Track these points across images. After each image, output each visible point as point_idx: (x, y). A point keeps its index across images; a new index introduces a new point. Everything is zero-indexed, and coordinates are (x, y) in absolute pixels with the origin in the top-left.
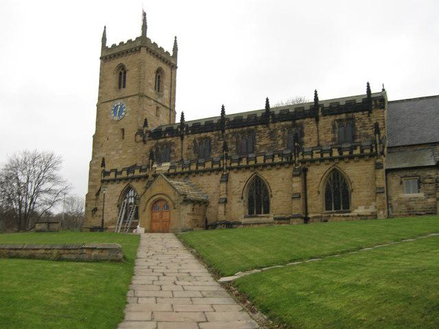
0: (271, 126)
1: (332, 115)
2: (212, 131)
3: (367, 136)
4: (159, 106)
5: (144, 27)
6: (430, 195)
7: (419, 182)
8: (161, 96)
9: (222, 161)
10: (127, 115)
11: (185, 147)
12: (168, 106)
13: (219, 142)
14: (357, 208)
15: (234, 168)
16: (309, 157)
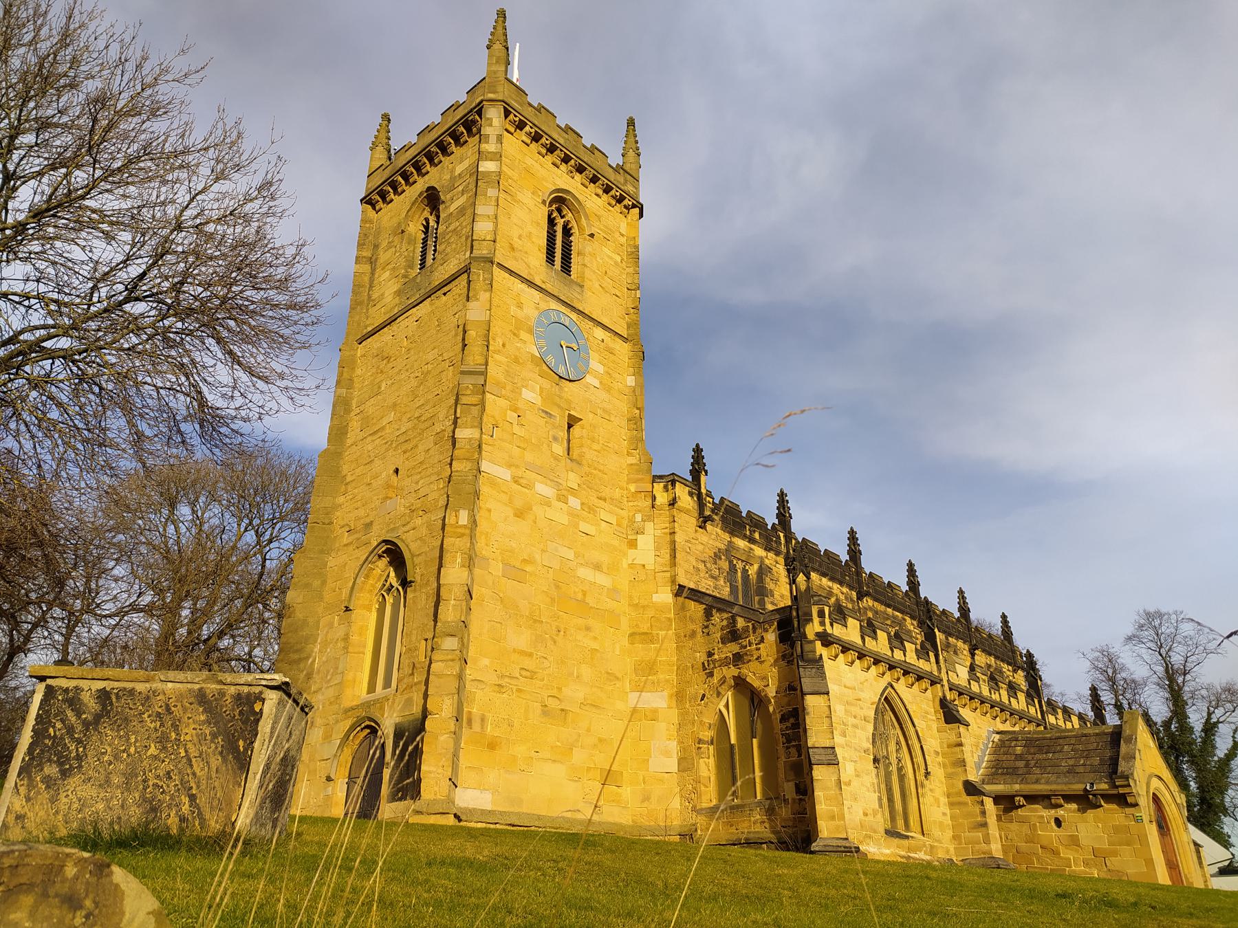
2: (841, 583)
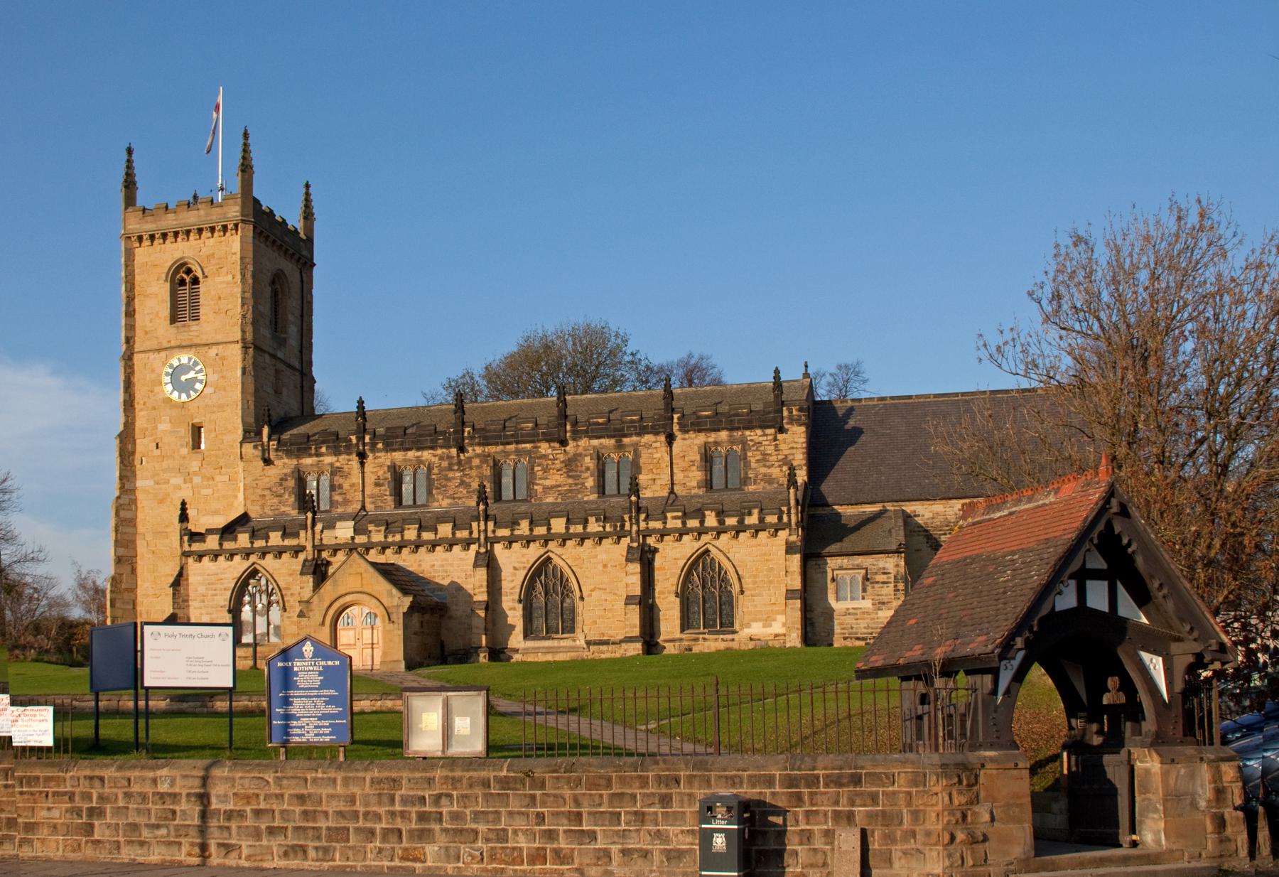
0: (572, 444)
1: (700, 431)
2: (433, 448)
3: (769, 480)
4: (281, 366)
5: (246, 168)
6: (884, 603)
7: (866, 578)
8: (282, 342)
9: (474, 525)
10: (209, 390)
11: (370, 479)
12: (297, 364)
13: (451, 475)
14: (748, 626)
15: (502, 538)
16: (656, 525)
